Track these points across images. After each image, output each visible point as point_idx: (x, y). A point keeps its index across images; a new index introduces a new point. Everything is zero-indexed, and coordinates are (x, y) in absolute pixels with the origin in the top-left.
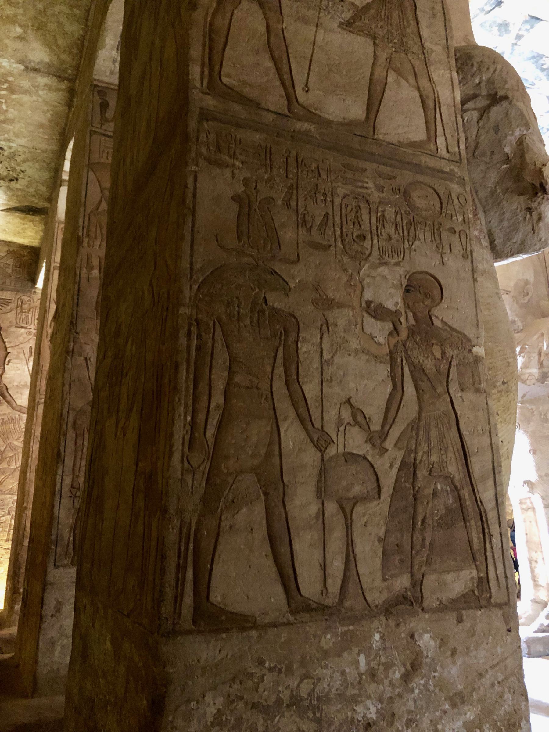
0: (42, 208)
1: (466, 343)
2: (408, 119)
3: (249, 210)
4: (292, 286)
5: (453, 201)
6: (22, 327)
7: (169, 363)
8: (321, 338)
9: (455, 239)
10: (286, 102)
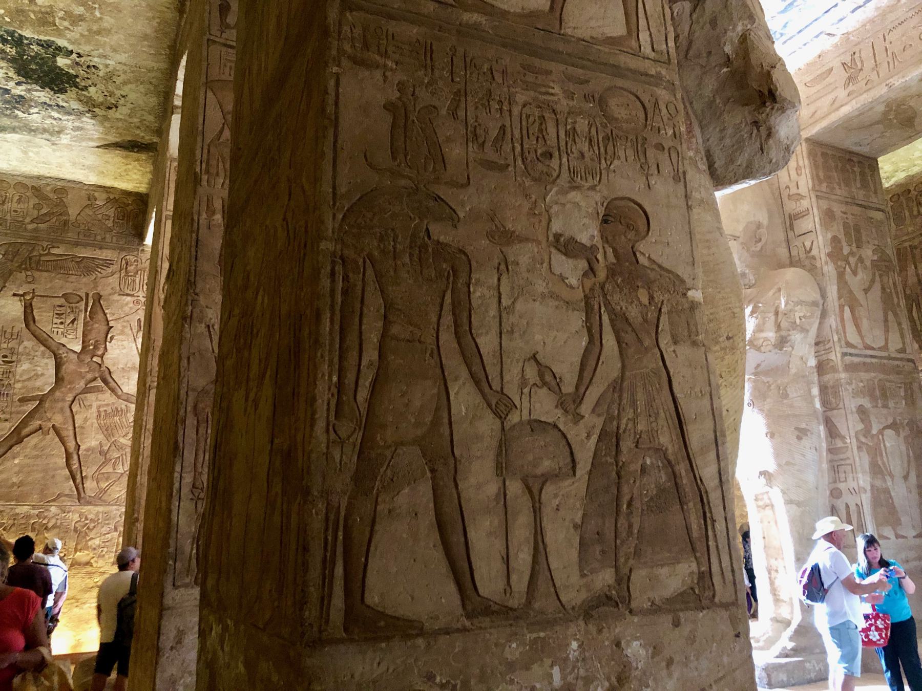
0: (149, 144)
1: (679, 285)
4: (461, 215)
6: (128, 295)
7: (308, 312)
8: (499, 280)
9: (663, 157)
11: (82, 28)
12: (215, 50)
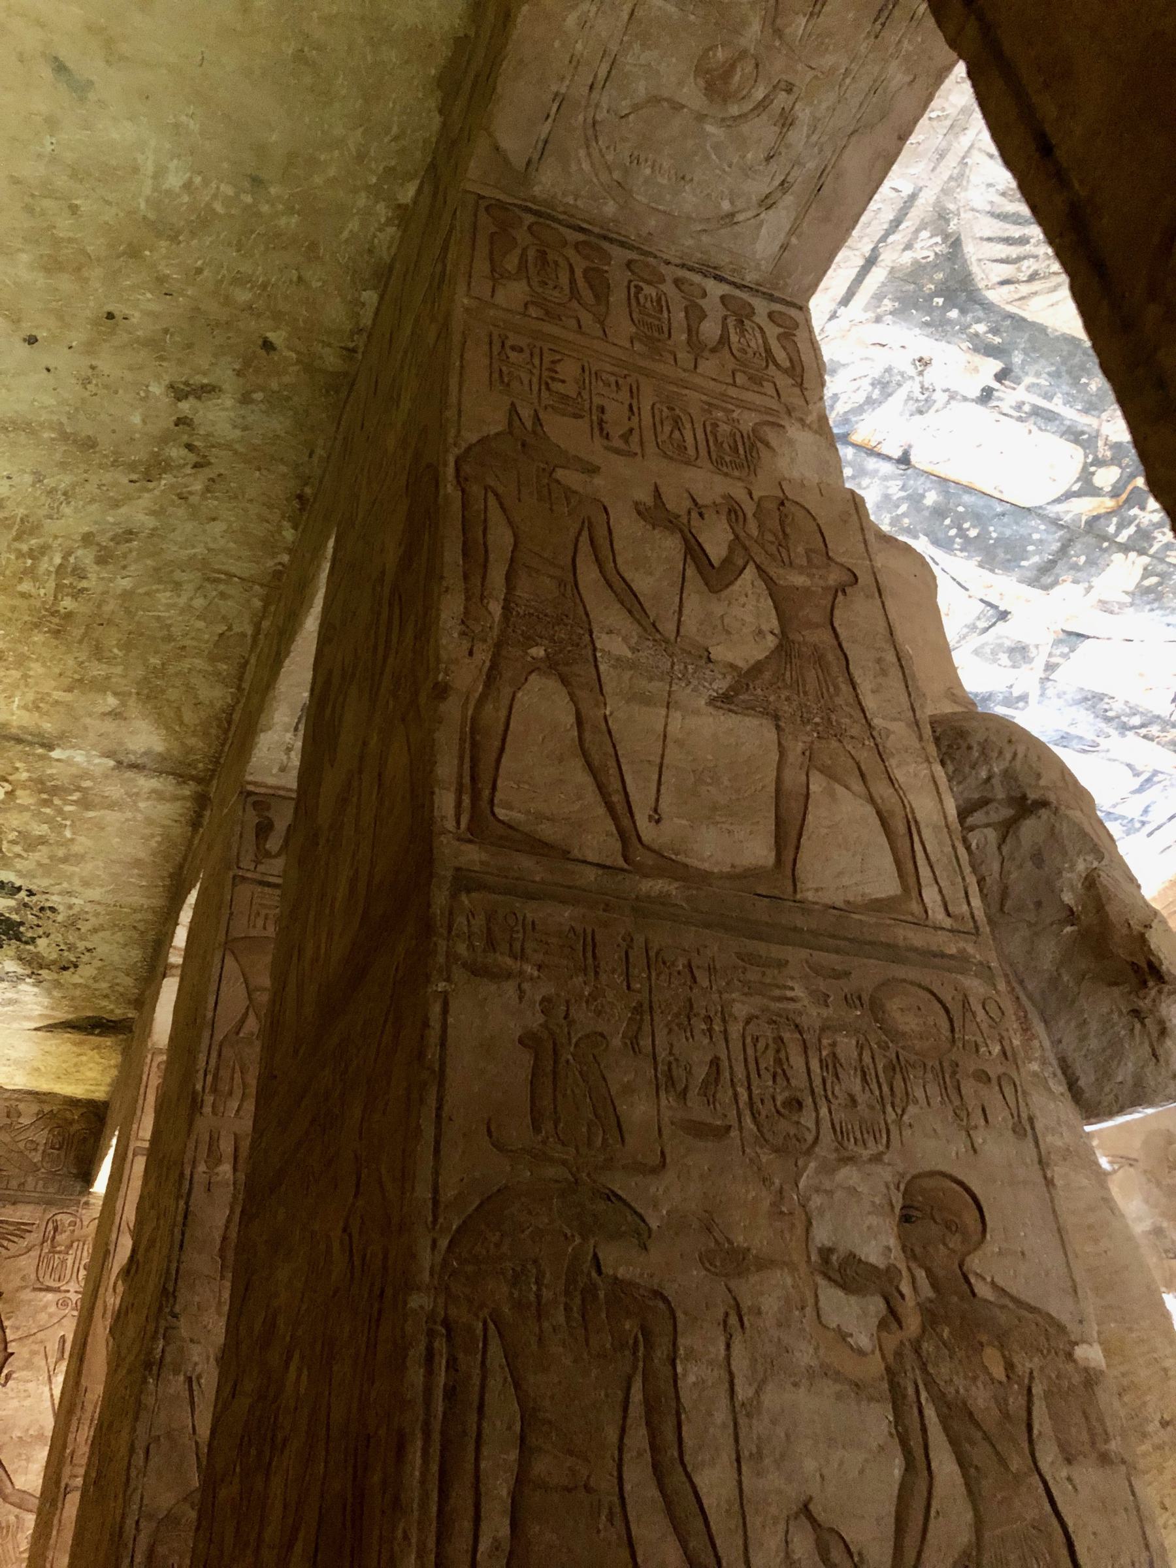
0: (120, 1021)
1: (1055, 1338)
2: (859, 858)
3: (556, 1062)
4: (654, 1224)
5: (974, 1015)
6: (49, 1289)
7: (382, 1432)
8: (728, 1346)
10: (619, 845)
11: (41, 854)
12: (245, 891)
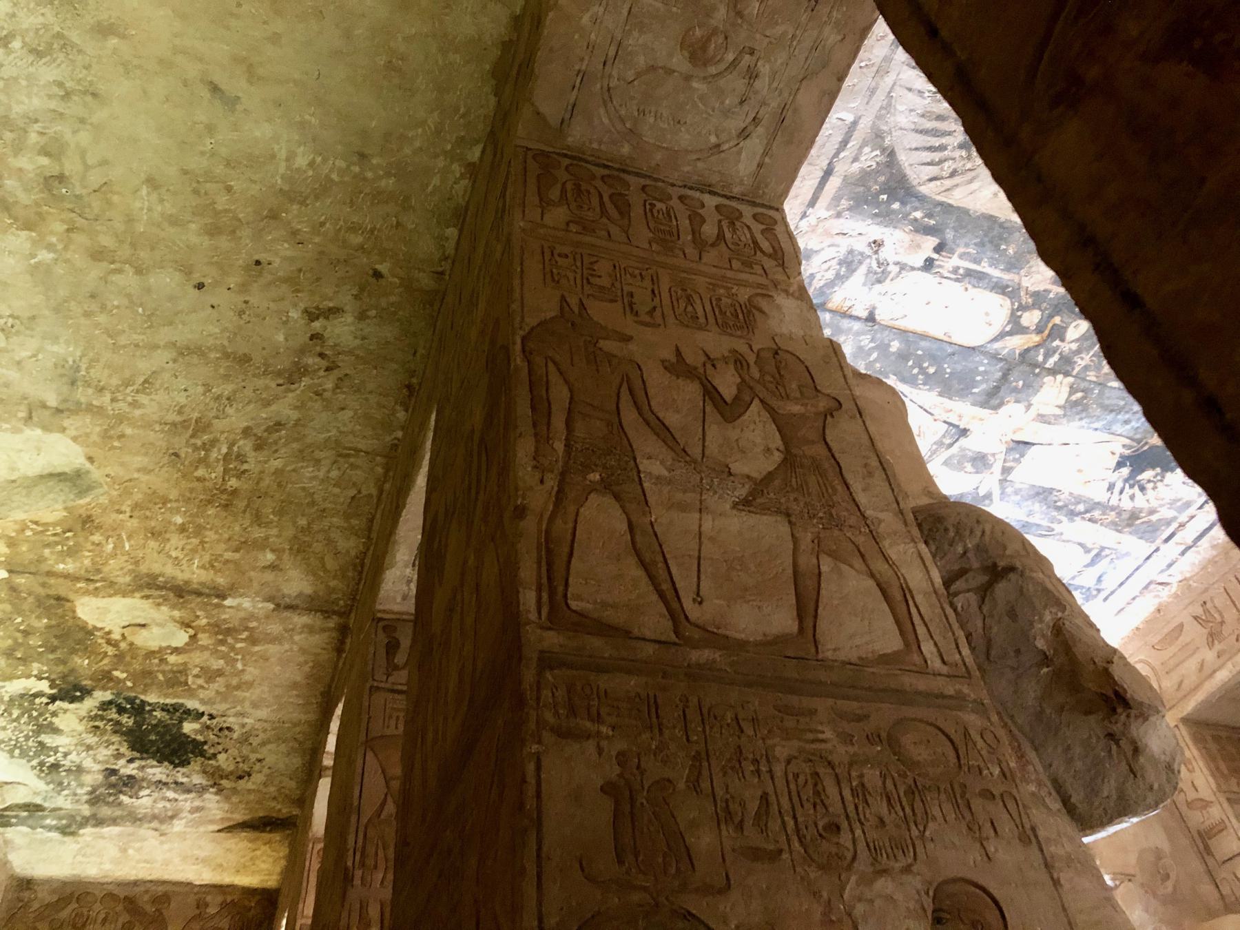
2: (866, 622)
3: (632, 806)
5: (975, 744)
9: (996, 810)
10: (670, 623)
11: (219, 685)
12: (379, 698)
